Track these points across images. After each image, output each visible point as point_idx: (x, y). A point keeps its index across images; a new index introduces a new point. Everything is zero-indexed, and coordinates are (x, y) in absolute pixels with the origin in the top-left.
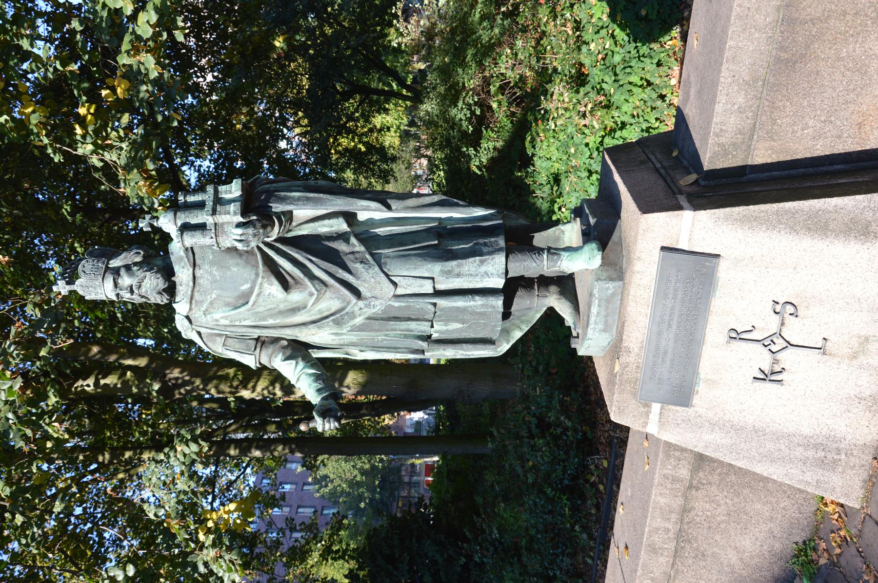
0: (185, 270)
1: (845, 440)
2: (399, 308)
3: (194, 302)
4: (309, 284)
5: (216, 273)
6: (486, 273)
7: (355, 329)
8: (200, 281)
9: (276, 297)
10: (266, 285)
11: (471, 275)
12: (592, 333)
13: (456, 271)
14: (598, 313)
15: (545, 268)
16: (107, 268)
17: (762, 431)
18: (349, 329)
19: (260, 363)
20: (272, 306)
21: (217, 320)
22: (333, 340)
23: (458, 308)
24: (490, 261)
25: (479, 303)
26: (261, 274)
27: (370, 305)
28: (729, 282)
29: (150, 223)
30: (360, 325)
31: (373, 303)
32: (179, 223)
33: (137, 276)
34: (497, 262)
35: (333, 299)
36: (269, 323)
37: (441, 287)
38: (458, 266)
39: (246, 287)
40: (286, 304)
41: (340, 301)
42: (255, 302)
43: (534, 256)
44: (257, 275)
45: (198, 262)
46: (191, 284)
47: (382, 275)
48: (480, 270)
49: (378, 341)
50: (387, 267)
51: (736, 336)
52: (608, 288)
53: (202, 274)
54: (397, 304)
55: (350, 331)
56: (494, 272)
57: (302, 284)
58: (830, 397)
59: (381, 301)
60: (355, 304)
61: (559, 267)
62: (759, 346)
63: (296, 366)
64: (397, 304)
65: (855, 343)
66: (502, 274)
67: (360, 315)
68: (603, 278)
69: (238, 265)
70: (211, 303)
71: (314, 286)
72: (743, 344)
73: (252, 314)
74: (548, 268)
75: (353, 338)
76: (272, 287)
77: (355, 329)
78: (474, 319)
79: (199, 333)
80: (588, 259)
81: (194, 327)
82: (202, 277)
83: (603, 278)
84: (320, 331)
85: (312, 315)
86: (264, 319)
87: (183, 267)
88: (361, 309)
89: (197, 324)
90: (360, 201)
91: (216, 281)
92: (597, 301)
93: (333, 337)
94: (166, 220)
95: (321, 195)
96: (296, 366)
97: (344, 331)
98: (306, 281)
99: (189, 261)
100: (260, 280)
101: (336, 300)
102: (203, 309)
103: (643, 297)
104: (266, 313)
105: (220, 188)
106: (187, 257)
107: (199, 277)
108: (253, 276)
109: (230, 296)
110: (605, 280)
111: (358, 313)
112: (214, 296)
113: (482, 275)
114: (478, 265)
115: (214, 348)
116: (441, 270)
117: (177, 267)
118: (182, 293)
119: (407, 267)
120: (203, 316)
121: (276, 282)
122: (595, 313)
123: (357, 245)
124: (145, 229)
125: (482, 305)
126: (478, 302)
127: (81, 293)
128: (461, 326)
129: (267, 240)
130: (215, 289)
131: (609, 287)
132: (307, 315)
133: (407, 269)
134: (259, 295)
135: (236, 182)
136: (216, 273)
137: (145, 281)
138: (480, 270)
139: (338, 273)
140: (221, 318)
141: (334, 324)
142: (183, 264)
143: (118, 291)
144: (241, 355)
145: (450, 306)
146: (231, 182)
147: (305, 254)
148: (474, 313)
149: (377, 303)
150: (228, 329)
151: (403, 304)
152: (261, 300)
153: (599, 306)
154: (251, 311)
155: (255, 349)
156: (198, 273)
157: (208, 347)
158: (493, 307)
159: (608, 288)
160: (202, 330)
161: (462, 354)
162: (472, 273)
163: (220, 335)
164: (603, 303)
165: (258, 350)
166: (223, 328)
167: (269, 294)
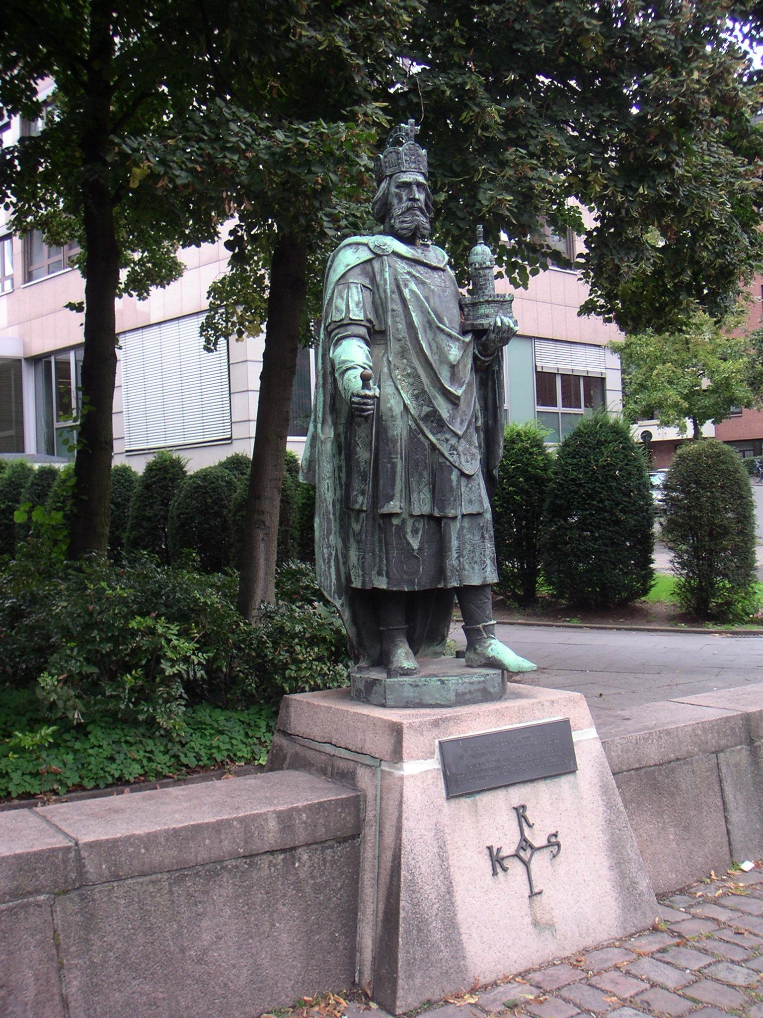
2: (450, 481)
13: (487, 536)
14: (472, 683)
21: (406, 286)
22: (391, 409)
51: (520, 812)
52: (494, 687)
54: (454, 476)
62: (517, 838)
65: (547, 917)
67: (438, 440)
72: (516, 823)
88: (447, 440)
140: (412, 291)
144: (361, 305)
153: (479, 682)
164: (481, 686)
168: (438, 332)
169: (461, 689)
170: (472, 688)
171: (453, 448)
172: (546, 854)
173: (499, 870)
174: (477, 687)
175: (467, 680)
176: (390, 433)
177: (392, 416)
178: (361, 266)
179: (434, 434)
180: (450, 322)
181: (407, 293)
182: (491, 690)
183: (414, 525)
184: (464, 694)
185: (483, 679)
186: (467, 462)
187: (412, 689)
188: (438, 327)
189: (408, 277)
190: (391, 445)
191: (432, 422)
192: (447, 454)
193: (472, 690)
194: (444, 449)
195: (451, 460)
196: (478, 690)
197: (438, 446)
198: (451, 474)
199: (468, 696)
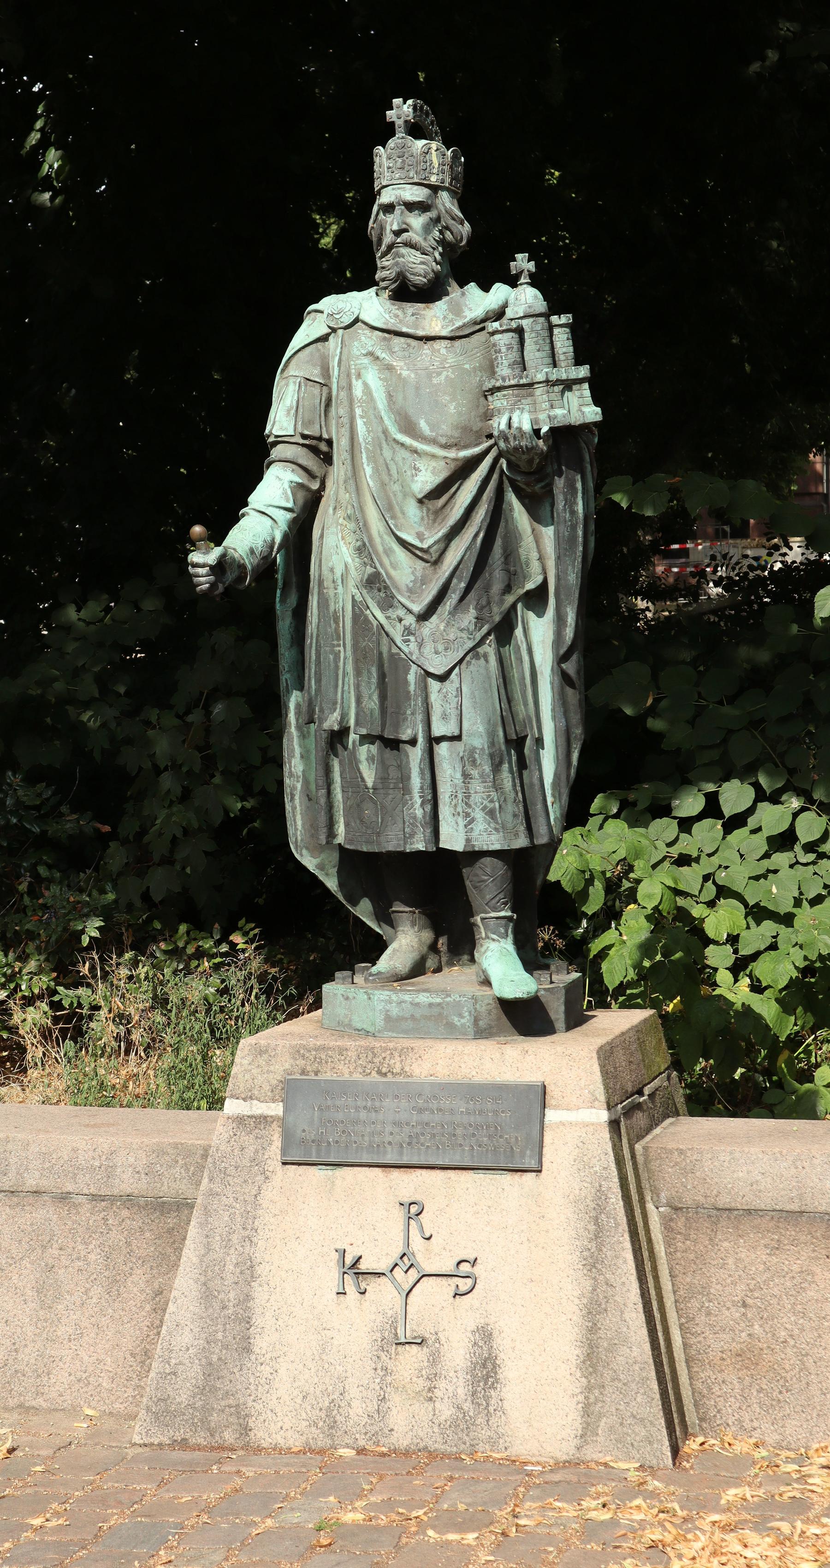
1: (254, 1401)
4: (440, 534)
5: (443, 377)
6: (473, 820)
8: (427, 349)
9: (413, 480)
10: (433, 463)
11: (468, 797)
12: (382, 997)
14: (417, 1005)
15: (483, 915)
16: (434, 189)
17: (252, 1277)
18: (358, 598)
19: (275, 444)
20: (394, 471)
21: (359, 376)
22: (332, 570)
23: (409, 778)
24: (492, 825)
26: (452, 454)
27: (408, 635)
28: (500, 1190)
29: (522, 271)
31: (412, 638)
32: (525, 323)
33: (425, 239)
34: (493, 837)
35: (413, 573)
36: (365, 466)
37: (443, 750)
38: (482, 776)
39: (424, 426)
40: (400, 496)
41: (411, 585)
43: (501, 896)
44: (446, 447)
45: (458, 343)
47: (461, 654)
48: (477, 810)
50: (473, 661)
52: (461, 1016)
53: (439, 350)
54: (411, 678)
56: (475, 834)
57: (434, 521)
58: (326, 1366)
60: (410, 611)
61: (487, 937)
66: (473, 846)
67: (388, 618)
68: (478, 1006)
69: (460, 414)
70: (390, 368)
71: (435, 543)
74: (483, 919)
76: (429, 474)
80: (510, 978)
82: (434, 351)
83: (478, 1006)
85: (381, 537)
86: (372, 459)
87: (445, 318)
88: (400, 620)
89: (346, 337)
90: (575, 611)
91: (429, 376)
92: (438, 1000)
94: (530, 300)
95: (581, 548)
98: (442, 531)
99: (459, 328)
100: (441, 453)
101: (413, 578)
102: (379, 353)
103: (463, 1066)
104: (381, 461)
105: (586, 386)
106: (464, 326)
107: (432, 345)
108: (443, 441)
110: (475, 1009)
111: (391, 613)
112: (405, 373)
113: (467, 815)
116: (475, 748)
119: (476, 693)
120: (364, 352)
122: (417, 1000)
123: (503, 609)
124: (512, 264)
125: (415, 818)
126: (418, 809)
127: (391, 143)
130: (416, 374)
131: (463, 1017)
133: (472, 693)
134: (415, 451)
136: (443, 377)
137: (418, 254)
138: (477, 810)
139: (460, 581)
140: (366, 385)
141: (370, 576)
142: (451, 316)
143: (398, 210)
144: (293, 412)
146: (596, 405)
147: (486, 524)
149: (413, 646)
150: (343, 394)
152: (405, 454)
153: (431, 1005)
154: (382, 436)
155: (304, 437)
156: (441, 345)
158: (412, 835)
159: (461, 1016)
164: (436, 1011)
165: (302, 441)
166: (343, 383)
167: (417, 469)
168: (397, 448)
169: (395, 1011)
171: (408, 631)
172: (447, 1287)
173: (351, 1288)
177: (334, 582)
180: (432, 427)
181: (358, 390)
186: (437, 653)
187: (344, 1002)
189: (366, 361)
191: (379, 590)
192: (398, 640)
193: (418, 1016)
194: (397, 634)
195: (406, 649)
197: (388, 627)
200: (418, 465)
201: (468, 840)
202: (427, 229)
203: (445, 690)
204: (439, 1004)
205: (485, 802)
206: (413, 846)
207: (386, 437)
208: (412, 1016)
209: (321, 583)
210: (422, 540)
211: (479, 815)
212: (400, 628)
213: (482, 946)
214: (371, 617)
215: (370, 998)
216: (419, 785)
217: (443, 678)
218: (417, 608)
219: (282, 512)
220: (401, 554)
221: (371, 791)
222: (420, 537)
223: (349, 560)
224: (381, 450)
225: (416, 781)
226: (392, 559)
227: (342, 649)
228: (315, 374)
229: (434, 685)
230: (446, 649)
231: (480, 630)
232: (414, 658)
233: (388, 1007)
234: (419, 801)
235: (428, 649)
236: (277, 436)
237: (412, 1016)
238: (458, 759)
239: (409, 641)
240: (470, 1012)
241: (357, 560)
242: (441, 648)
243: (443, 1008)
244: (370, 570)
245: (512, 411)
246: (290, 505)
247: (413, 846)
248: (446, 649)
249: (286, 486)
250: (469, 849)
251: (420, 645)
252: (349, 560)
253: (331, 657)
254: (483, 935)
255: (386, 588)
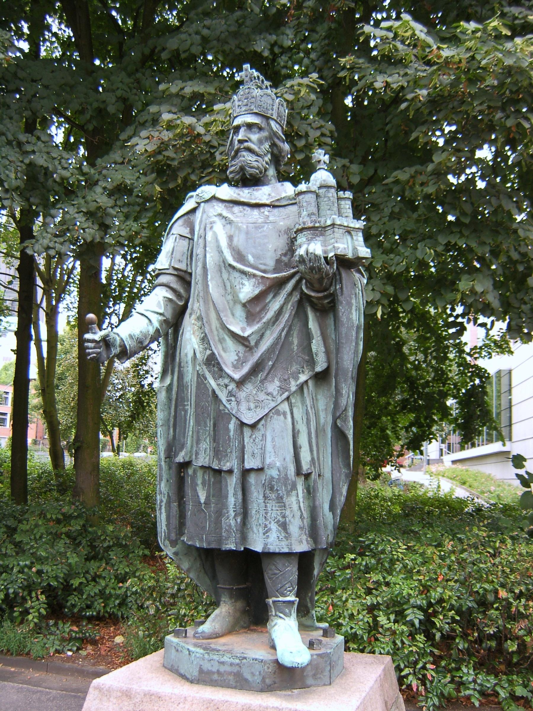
0: (266, 197)
2: (228, 430)
3: (231, 205)
7: (201, 378)
8: (255, 212)
14: (223, 663)
15: (275, 599)
20: (228, 287)
21: (211, 228)
22: (186, 355)
23: (227, 497)
25: (233, 522)
30: (205, 385)
31: (233, 399)
35: (237, 355)
37: (252, 479)
39: (250, 258)
42: (234, 268)
44: (264, 271)
46: (253, 202)
49: (185, 405)
52: (253, 674)
54: (232, 425)
55: (198, 374)
56: (270, 540)
59: (236, 408)
61: (276, 615)
63: (158, 313)
64: (232, 425)
66: (269, 548)
67: (218, 385)
70: (230, 222)
73: (220, 266)
74: (274, 602)
75: (190, 376)
77: (201, 378)
78: (210, 516)
79: (193, 211)
81: (202, 204)
84: (198, 340)
85: (217, 330)
87: (269, 195)
88: (226, 386)
93: (190, 355)
96: (158, 313)
97: (198, 368)
101: (237, 358)
105: (360, 234)
109: (239, 241)
111: (222, 382)
113: (266, 526)
114: (279, 521)
115: (176, 226)
116: (273, 478)
117: (270, 189)
118: (241, 193)
121: (257, 292)
122: (222, 660)
123: (298, 383)
125: (230, 525)
128: (202, 500)
129: (304, 281)
132: (218, 325)
135: (367, 252)
138: (273, 522)
144: (170, 254)
145: (229, 488)
148: (220, 514)
149: (234, 404)
150: (201, 241)
151: (232, 433)
153: (231, 664)
154: (223, 265)
157: (179, 218)
158: (227, 538)
160: (199, 213)
161: (161, 501)
162: (269, 514)
163: (192, 232)
164: (235, 669)
167: (243, 284)
168: (231, 270)
169: (207, 666)
170: (222, 669)
171: (231, 394)
174: (228, 668)
175: (216, 657)
176: (185, 381)
178: (186, 217)
179: (215, 379)
180: (257, 257)
181: (209, 236)
182: (249, 677)
183: (203, 477)
184: (210, 673)
185: (237, 661)
188: (230, 265)
190: (186, 392)
191: (214, 366)
192: (224, 400)
194: (223, 396)
195: (228, 406)
196: (230, 673)
197: (218, 392)
198: (229, 423)
199: (216, 677)
200: (244, 282)
201: (266, 544)
202: (260, 142)
203: (254, 436)
204: (238, 664)
205: (278, 517)
206: (227, 546)
207: (225, 264)
208: (218, 671)
209: (180, 364)
210: (243, 332)
211: (274, 527)
212: (225, 392)
213: (272, 621)
214: (208, 385)
215: (190, 654)
216: (233, 503)
217: (253, 426)
218: (237, 376)
219: (156, 315)
220: (230, 343)
221: (203, 505)
222: (243, 330)
223: (196, 347)
224: (221, 273)
225: (231, 500)
226: (224, 345)
227: (189, 407)
228: (185, 232)
229: (247, 432)
230: (256, 407)
231: (281, 395)
232: (234, 412)
233: (202, 663)
234: (233, 514)
235: (243, 407)
236: (160, 270)
237: (218, 671)
238: (261, 485)
239: (231, 400)
240: (260, 672)
241: (201, 346)
242: (252, 406)
243: (240, 667)
244: (208, 352)
245: (309, 244)
246: (161, 311)
247: (227, 546)
248: (256, 407)
249: (161, 300)
250: (266, 551)
251: (238, 403)
252: (196, 347)
253: (183, 413)
254: (274, 614)
255: (219, 364)
